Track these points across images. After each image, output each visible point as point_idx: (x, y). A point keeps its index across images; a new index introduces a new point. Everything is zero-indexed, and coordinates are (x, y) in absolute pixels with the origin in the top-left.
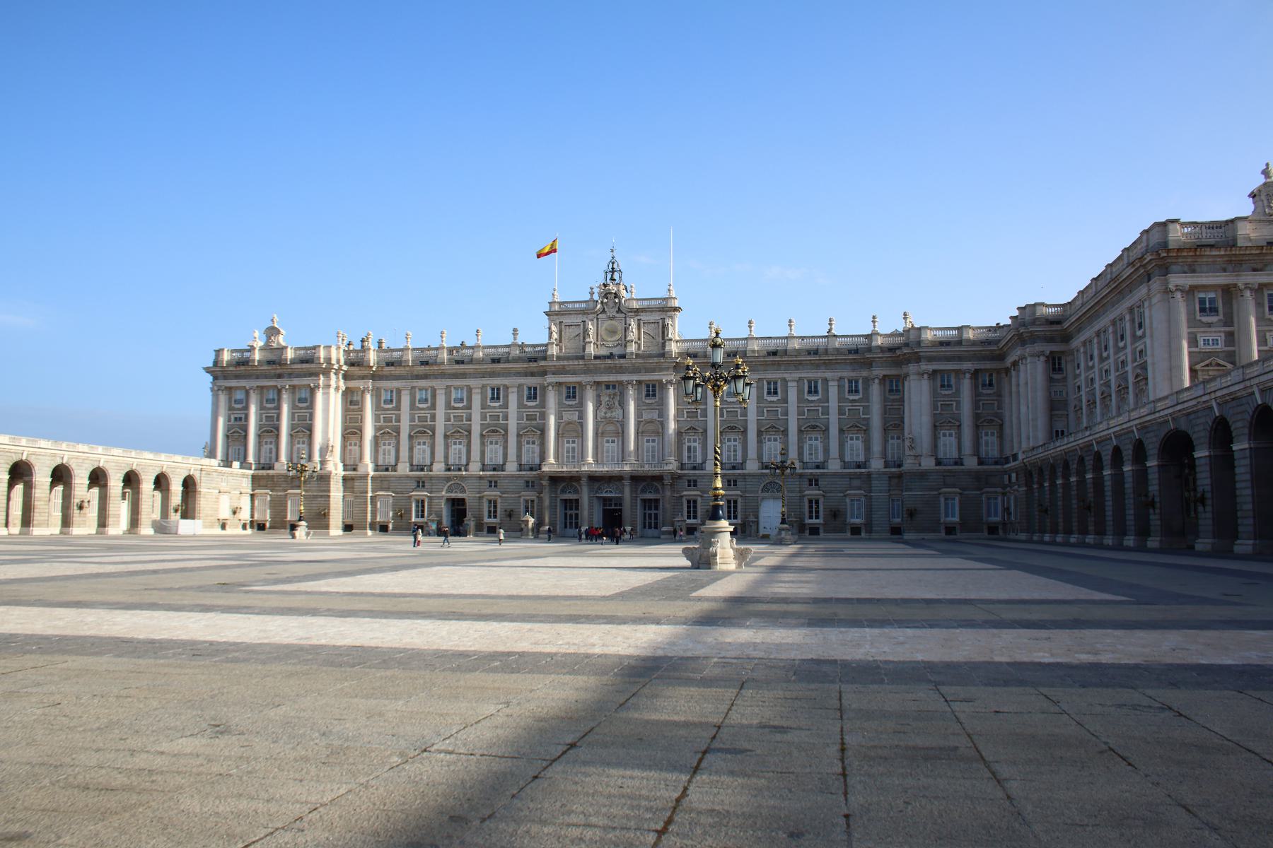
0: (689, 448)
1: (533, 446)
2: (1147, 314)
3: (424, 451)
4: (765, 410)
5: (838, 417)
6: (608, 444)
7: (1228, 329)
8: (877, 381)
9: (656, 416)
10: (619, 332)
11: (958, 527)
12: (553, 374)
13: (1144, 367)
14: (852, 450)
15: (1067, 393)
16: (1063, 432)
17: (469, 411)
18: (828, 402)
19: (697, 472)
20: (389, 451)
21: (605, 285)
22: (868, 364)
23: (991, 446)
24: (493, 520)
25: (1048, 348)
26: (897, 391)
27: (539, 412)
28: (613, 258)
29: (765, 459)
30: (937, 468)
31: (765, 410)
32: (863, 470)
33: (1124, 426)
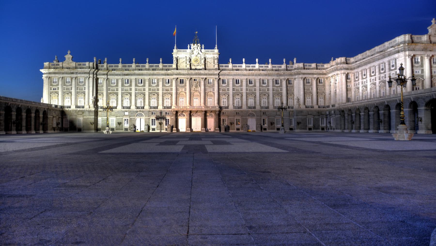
0: (223, 102)
1: (168, 100)
3: (127, 101)
5: (272, 91)
6: (195, 100)
8: (285, 80)
9: (212, 90)
10: (199, 61)
12: (176, 75)
14: (277, 102)
15: (351, 86)
17: (144, 87)
18: (269, 87)
19: (226, 109)
20: (114, 101)
23: (321, 103)
24: (154, 126)
25: (347, 72)
26: (291, 84)
27: (171, 88)
29: (249, 105)
30: (306, 109)
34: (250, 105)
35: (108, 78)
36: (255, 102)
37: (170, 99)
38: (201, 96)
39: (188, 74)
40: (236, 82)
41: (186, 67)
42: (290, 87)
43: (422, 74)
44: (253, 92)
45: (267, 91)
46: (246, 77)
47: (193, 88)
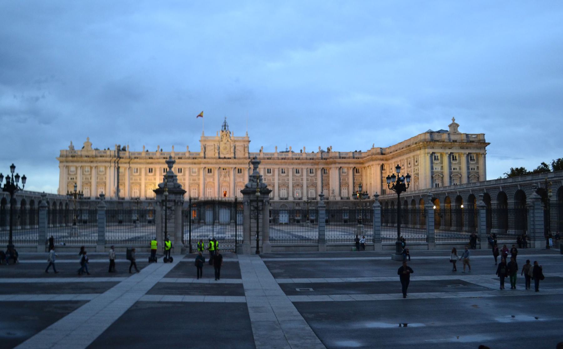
2: (419, 159)
4: (281, 179)
7: (441, 165)
11: (348, 221)
12: (204, 164)
13: (418, 174)
16: (385, 190)
18: (303, 176)
21: (223, 131)
22: (317, 164)
25: (381, 163)
26: (327, 173)
28: (225, 121)
29: (281, 196)
30: (342, 200)
31: (281, 179)
32: (315, 201)
33: (417, 194)
34: (282, 195)
35: (130, 167)
36: (288, 193)
37: (197, 189)
38: (230, 186)
39: (216, 163)
40: (268, 171)
41: (214, 155)
42: (325, 176)
43: (442, 171)
44: (286, 182)
45: (301, 181)
46: (278, 167)
47: (222, 178)
